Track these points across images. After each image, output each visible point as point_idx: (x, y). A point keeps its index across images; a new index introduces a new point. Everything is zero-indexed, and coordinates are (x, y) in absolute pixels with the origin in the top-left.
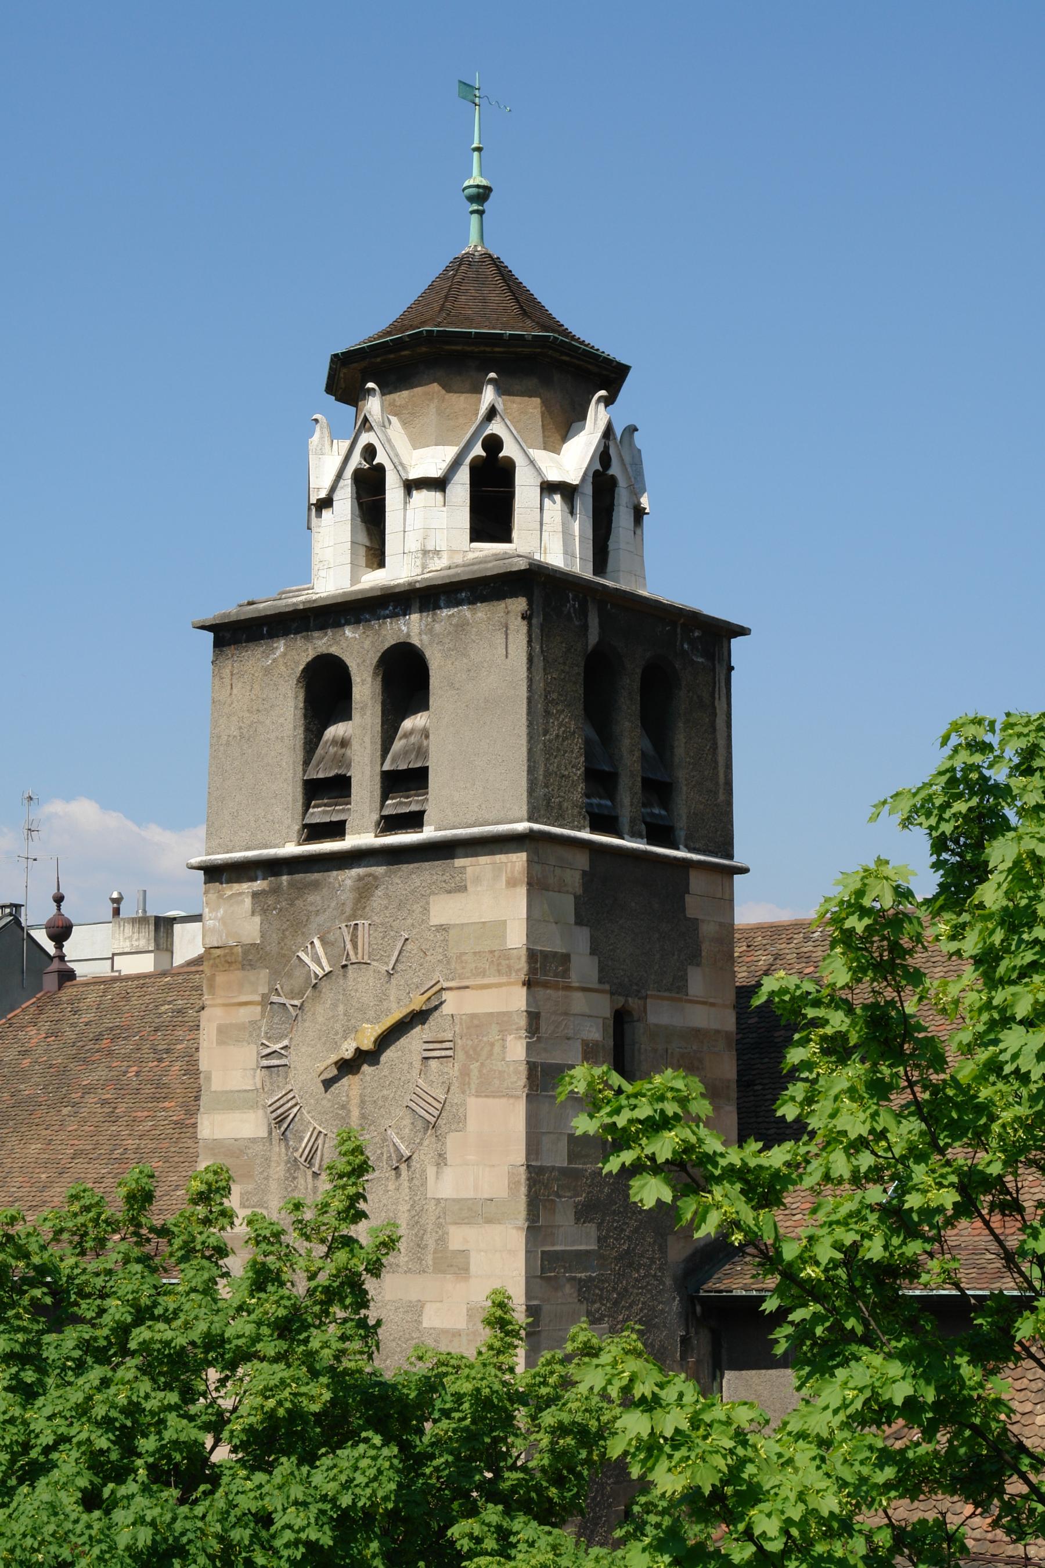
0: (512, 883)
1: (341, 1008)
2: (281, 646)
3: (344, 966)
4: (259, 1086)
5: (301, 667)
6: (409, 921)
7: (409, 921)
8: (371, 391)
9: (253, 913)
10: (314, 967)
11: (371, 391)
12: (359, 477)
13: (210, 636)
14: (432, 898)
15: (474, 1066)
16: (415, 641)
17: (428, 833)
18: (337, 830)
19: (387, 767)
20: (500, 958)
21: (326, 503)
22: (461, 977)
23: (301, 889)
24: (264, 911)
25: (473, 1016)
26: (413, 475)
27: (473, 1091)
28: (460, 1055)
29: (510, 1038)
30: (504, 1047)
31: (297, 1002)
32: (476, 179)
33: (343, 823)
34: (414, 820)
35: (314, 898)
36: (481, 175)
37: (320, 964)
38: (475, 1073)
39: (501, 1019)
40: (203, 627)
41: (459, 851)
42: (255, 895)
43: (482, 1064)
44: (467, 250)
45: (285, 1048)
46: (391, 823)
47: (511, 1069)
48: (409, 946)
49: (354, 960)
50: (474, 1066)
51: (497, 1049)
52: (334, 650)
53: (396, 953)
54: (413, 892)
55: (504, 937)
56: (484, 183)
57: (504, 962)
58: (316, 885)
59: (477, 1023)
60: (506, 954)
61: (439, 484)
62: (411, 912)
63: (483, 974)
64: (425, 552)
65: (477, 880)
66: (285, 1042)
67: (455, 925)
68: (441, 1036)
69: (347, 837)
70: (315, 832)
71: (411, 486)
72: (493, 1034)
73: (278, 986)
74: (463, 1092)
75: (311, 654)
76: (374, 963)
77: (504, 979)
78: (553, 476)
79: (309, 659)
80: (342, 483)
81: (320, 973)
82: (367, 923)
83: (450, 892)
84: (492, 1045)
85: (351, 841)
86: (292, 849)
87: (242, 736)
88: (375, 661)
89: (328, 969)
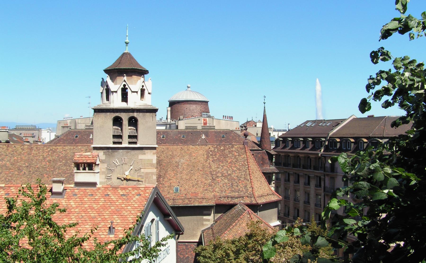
0: (154, 154)
1: (122, 170)
2: (108, 114)
3: (122, 164)
4: (106, 181)
5: (113, 117)
6: (135, 158)
7: (135, 158)
8: (125, 76)
9: (104, 155)
10: (116, 164)
11: (125, 76)
12: (122, 89)
13: (93, 110)
14: (139, 155)
15: (147, 179)
16: (136, 116)
17: (138, 146)
18: (121, 143)
19: (129, 134)
20: (152, 165)
21: (116, 92)
22: (144, 167)
23: (114, 152)
24: (106, 155)
25: (147, 172)
26: (133, 90)
27: (147, 183)
28: (144, 178)
29: (153, 176)
30: (152, 177)
31: (113, 169)
32: (127, 41)
33: (122, 142)
34: (135, 143)
35: (116, 153)
36: (128, 40)
37: (117, 162)
38: (147, 181)
39: (152, 174)
40: (93, 109)
41: (144, 148)
42: (104, 152)
43: (148, 179)
44: (126, 52)
45: (111, 176)
46: (130, 143)
47: (154, 180)
48: (135, 162)
49: (124, 163)
50: (147, 179)
51: (151, 177)
52: (119, 116)
53: (132, 163)
54: (135, 154)
55: (152, 162)
56: (128, 41)
57: (152, 165)
58: (117, 152)
59: (147, 174)
60: (153, 164)
61: (137, 92)
62: (135, 157)
63: (148, 166)
64: (135, 102)
65: (147, 153)
66: (111, 175)
67: (143, 159)
68: (141, 175)
69: (122, 144)
70: (114, 143)
71: (132, 92)
72: (150, 175)
73: (109, 166)
74: (145, 183)
75: (115, 116)
76: (128, 164)
77: (152, 167)
78: (149, 92)
79: (114, 116)
80: (119, 89)
81: (118, 165)
82: (127, 158)
83: (142, 154)
84: (150, 177)
85: (123, 145)
86: (112, 145)
87: (100, 127)
88: (128, 118)
89: (119, 164)
